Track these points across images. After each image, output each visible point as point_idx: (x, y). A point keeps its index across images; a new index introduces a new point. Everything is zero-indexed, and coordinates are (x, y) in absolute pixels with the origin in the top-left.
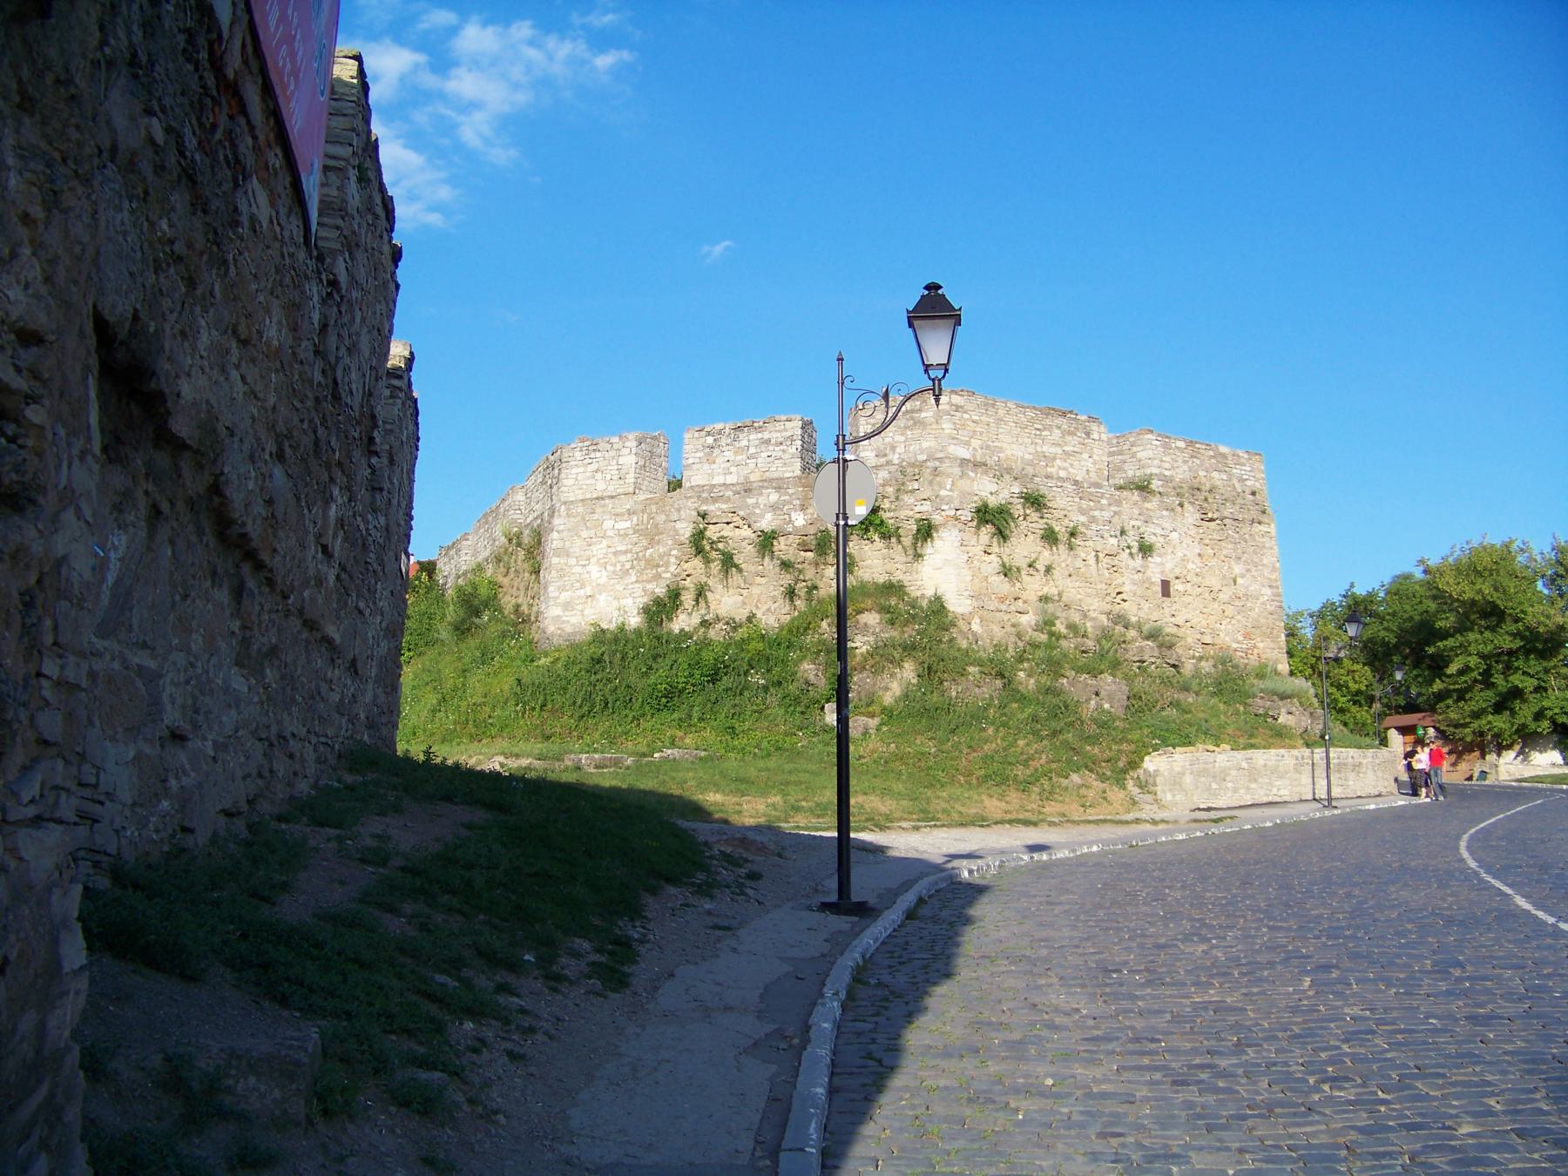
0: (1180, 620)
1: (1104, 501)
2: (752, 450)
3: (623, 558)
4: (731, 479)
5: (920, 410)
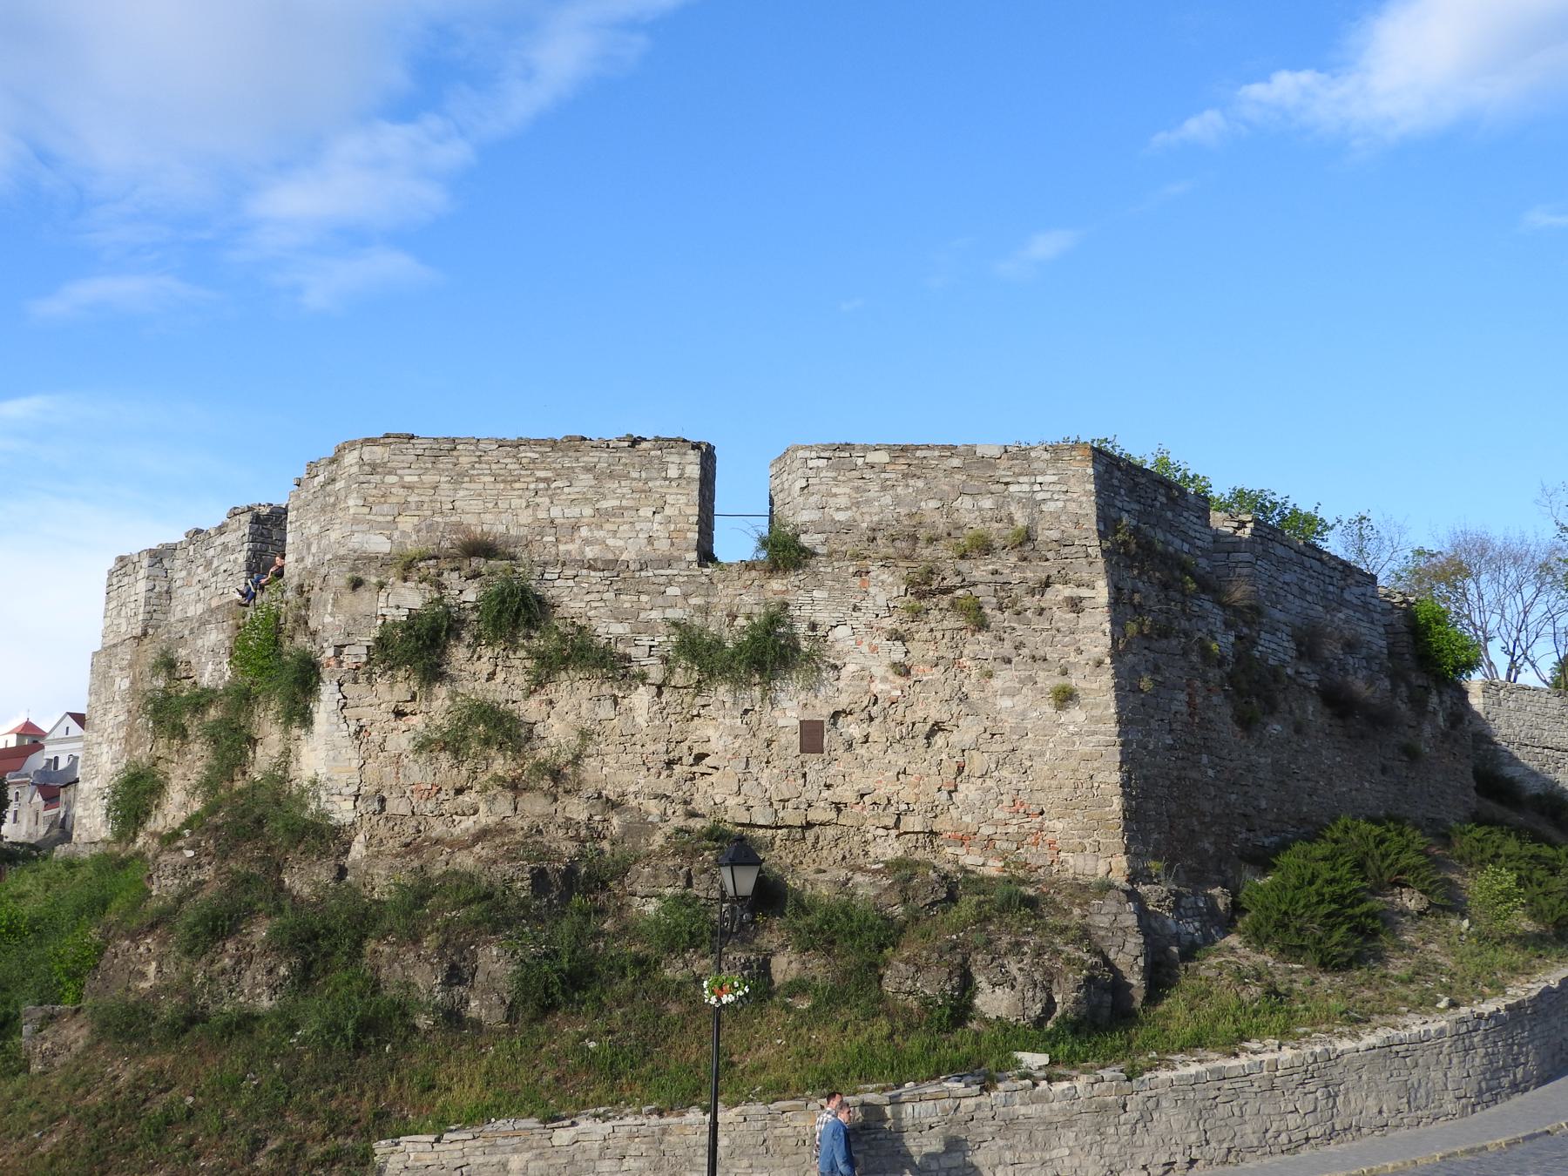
0: (845, 793)
1: (673, 591)
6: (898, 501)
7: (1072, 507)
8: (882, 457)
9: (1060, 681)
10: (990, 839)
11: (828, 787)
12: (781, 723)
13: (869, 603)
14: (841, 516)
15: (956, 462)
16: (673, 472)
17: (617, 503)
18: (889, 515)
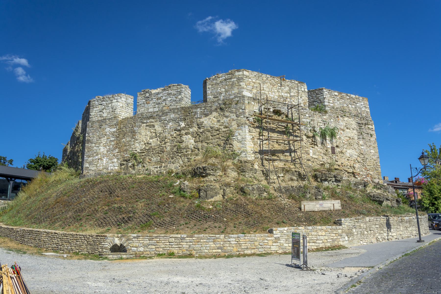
0: (339, 163)
2: (164, 98)
3: (113, 143)
4: (156, 109)
5: (231, 79)
11: (337, 161)
12: (328, 147)
14: (332, 105)
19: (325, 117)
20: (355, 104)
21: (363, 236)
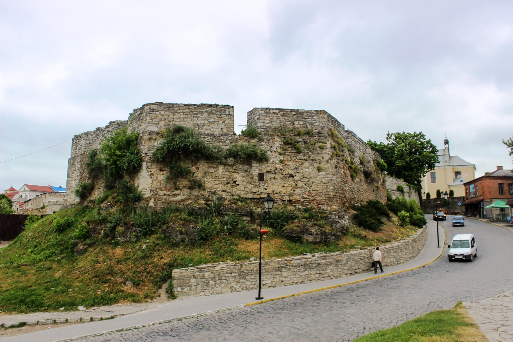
0: (269, 191)
1: (228, 142)
5: (142, 113)
6: (281, 122)
7: (321, 124)
8: (277, 111)
9: (318, 165)
10: (303, 202)
11: (266, 189)
12: (254, 174)
13: (274, 146)
15: (294, 113)
16: (227, 113)
17: (213, 120)
18: (279, 125)
19: (252, 141)
20: (303, 119)
21: (205, 287)
